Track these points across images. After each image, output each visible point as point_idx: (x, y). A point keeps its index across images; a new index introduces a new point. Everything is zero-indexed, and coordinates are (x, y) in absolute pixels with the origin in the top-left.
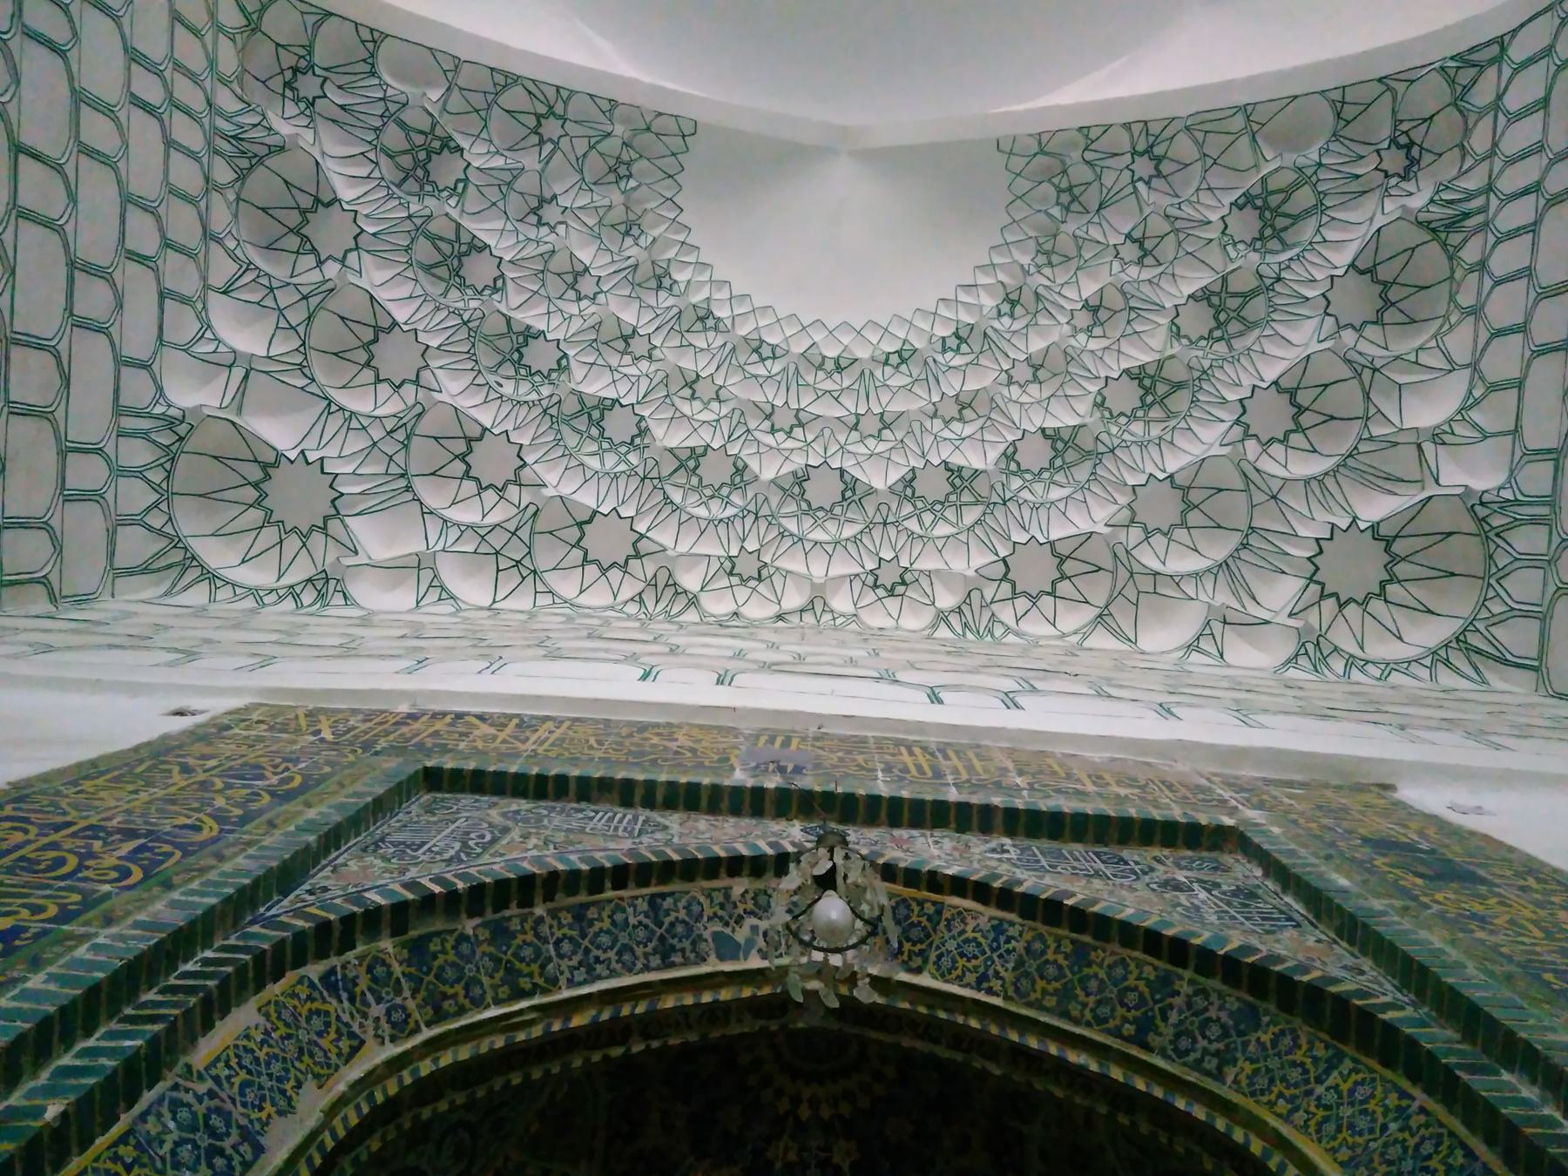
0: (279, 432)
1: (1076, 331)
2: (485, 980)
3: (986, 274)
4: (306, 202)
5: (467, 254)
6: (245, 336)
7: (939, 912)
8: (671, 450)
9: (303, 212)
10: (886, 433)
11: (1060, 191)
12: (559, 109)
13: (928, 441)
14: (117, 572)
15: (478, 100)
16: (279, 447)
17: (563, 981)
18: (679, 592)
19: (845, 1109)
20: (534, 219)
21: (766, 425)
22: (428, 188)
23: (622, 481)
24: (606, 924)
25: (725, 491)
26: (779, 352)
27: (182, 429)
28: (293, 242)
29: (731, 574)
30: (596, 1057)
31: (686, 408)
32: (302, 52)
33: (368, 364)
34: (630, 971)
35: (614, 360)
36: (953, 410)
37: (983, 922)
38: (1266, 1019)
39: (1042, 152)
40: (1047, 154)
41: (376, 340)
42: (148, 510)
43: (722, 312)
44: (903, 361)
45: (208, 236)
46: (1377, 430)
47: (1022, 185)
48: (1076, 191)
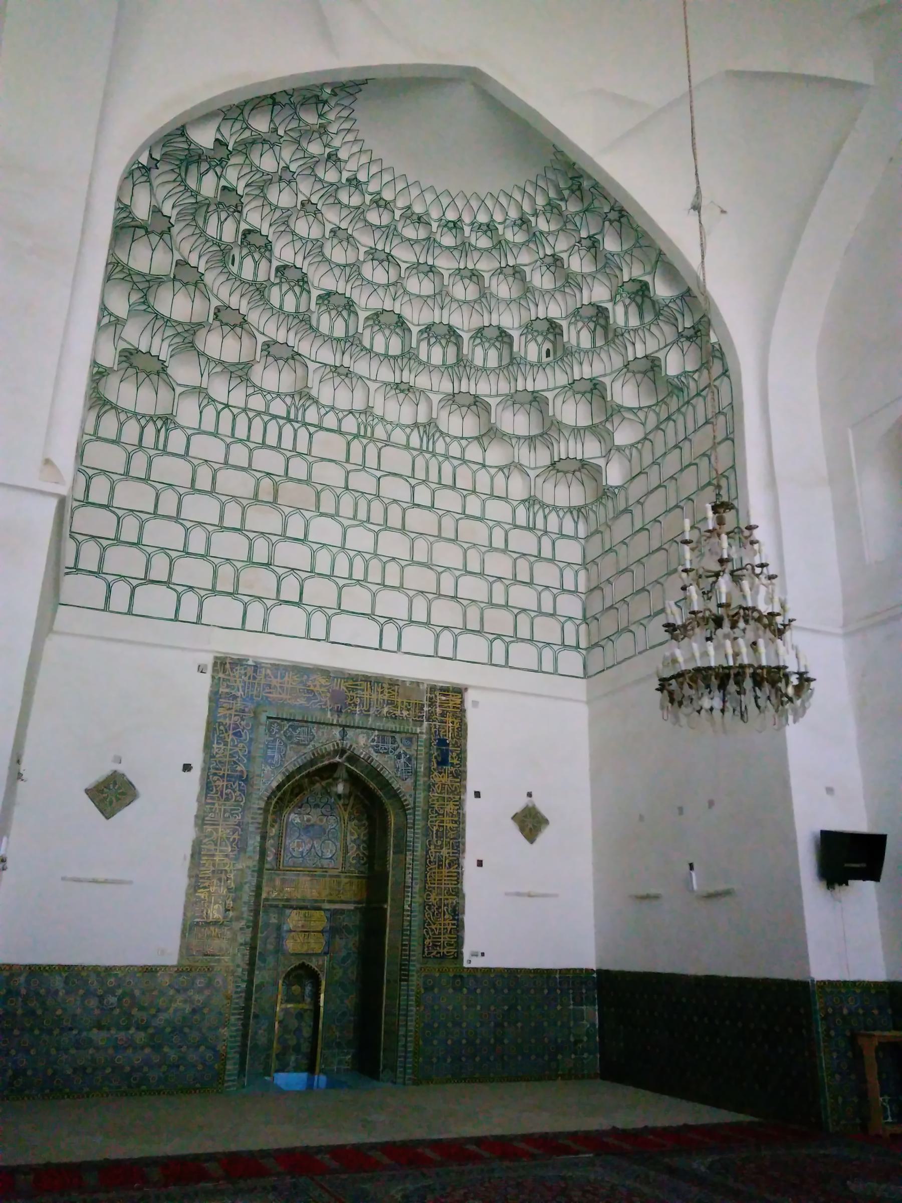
10: (431, 274)
11: (573, 184)
18: (310, 397)
21: (371, 256)
23: (291, 318)
25: (340, 309)
43: (362, 177)
46: (609, 426)
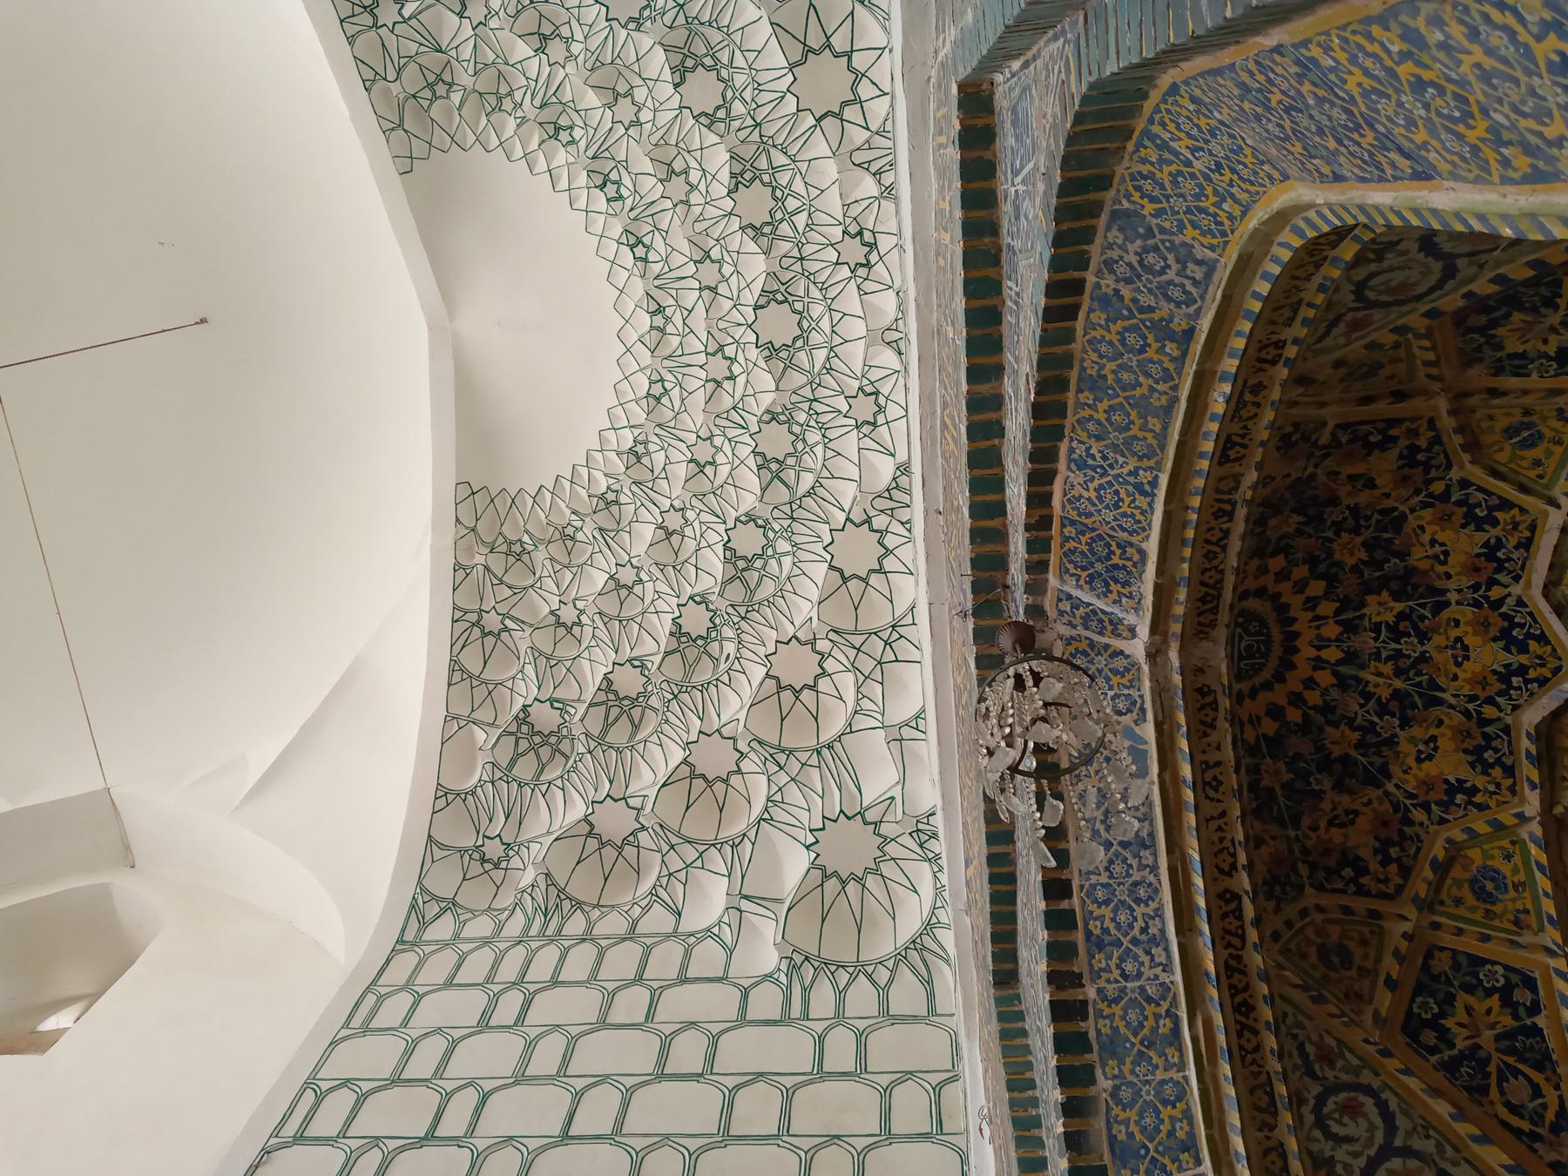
0: (795, 865)
1: (571, 57)
2: (1160, 1075)
3: (535, 162)
4: (593, 844)
5: (616, 693)
6: (710, 899)
7: (1073, 523)
8: (764, 490)
9: (602, 845)
11: (435, 97)
12: (473, 617)
13: (711, 212)
14: (932, 1010)
15: (480, 693)
16: (806, 866)
17: (1164, 977)
19: (1327, 608)
20: (576, 630)
21: (727, 385)
22: (565, 732)
24: (1106, 911)
25: (796, 429)
26: (655, 377)
27: (798, 959)
28: (629, 851)
29: (874, 424)
30: (1253, 935)
31: (724, 471)
32: (467, 857)
33: (726, 781)
34: (1156, 891)
35: (691, 545)
36: (678, 184)
37: (1077, 478)
38: (1126, 204)
39: (401, 125)
40: (402, 119)
41: (703, 776)
42: (874, 983)
44: (639, 241)
45: (631, 935)
47: (440, 138)
48: (431, 78)
